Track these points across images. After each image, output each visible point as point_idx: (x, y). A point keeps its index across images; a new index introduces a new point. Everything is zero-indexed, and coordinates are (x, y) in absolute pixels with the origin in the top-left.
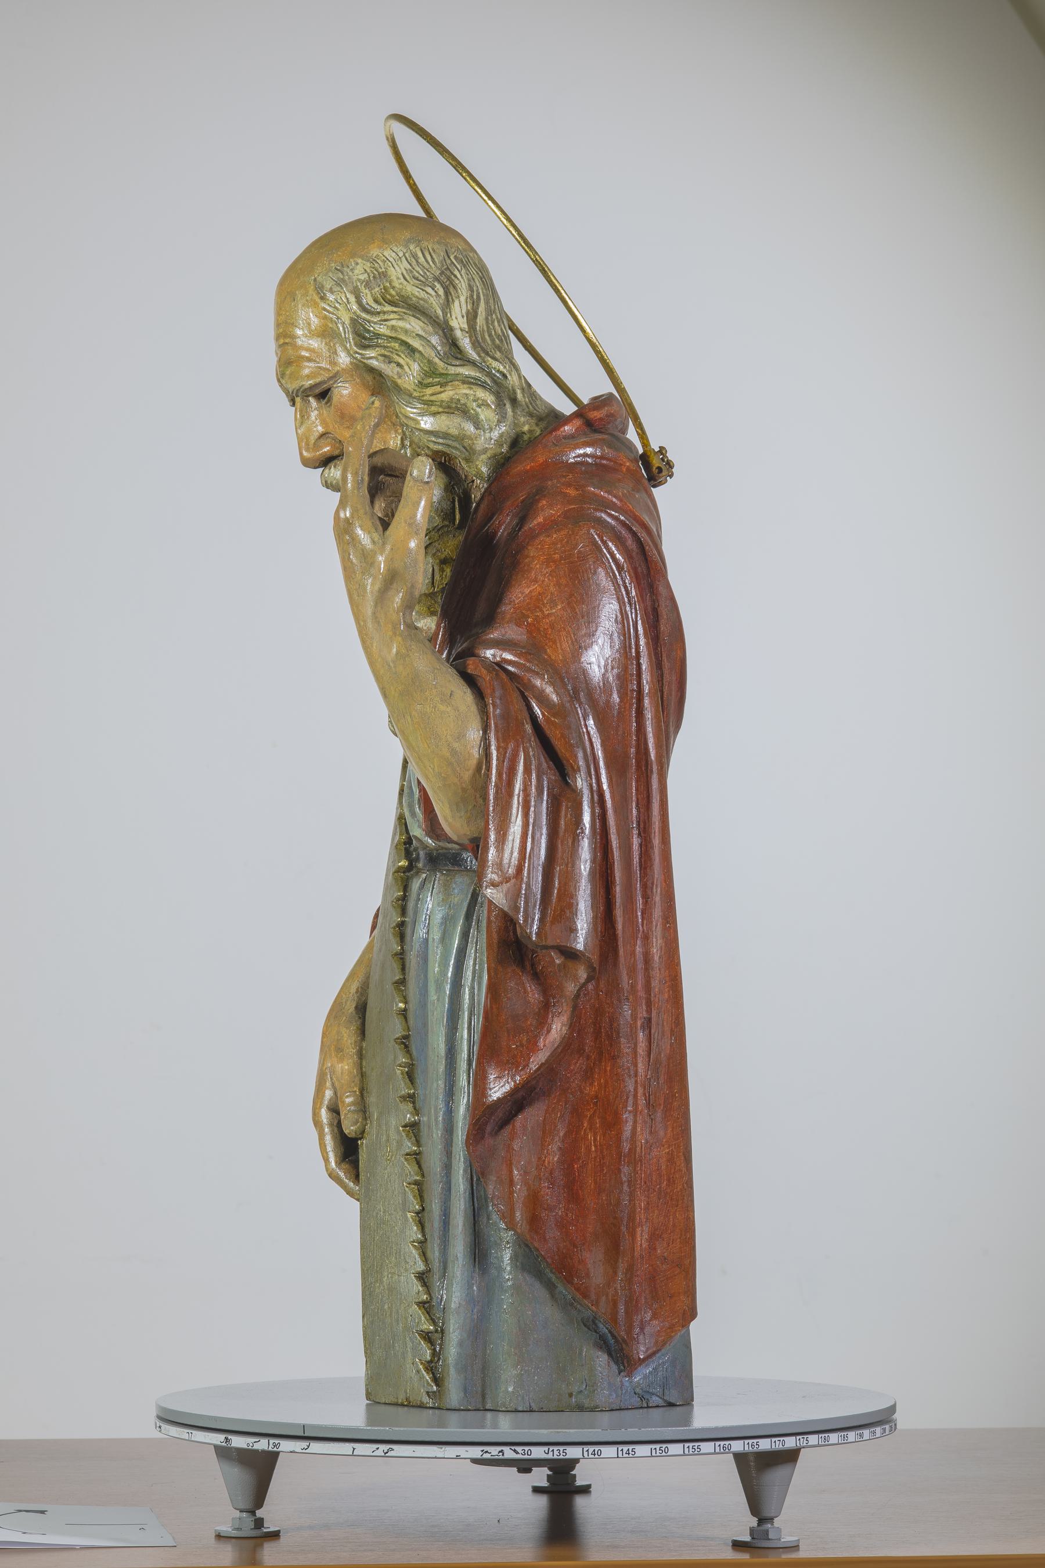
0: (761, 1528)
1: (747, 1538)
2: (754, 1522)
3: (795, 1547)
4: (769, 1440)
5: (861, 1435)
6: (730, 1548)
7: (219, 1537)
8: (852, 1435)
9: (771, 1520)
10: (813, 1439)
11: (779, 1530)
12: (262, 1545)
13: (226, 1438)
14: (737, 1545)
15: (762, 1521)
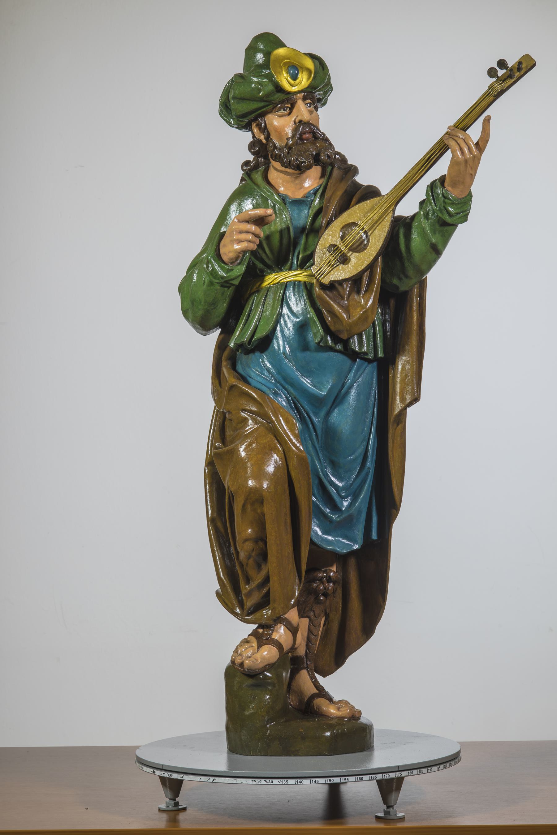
0: (389, 810)
1: (382, 815)
2: (385, 807)
3: (402, 819)
4: (381, 775)
5: (431, 770)
6: (374, 819)
7: (160, 810)
8: (425, 770)
9: (392, 807)
10: (404, 773)
11: (396, 811)
12: (178, 814)
13: (154, 772)
14: (377, 817)
15: (388, 807)
